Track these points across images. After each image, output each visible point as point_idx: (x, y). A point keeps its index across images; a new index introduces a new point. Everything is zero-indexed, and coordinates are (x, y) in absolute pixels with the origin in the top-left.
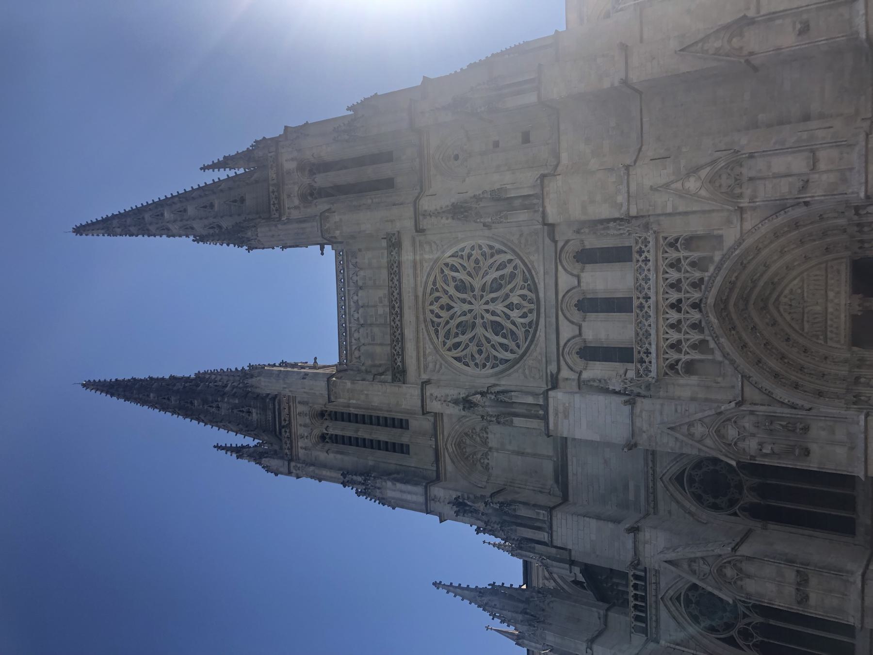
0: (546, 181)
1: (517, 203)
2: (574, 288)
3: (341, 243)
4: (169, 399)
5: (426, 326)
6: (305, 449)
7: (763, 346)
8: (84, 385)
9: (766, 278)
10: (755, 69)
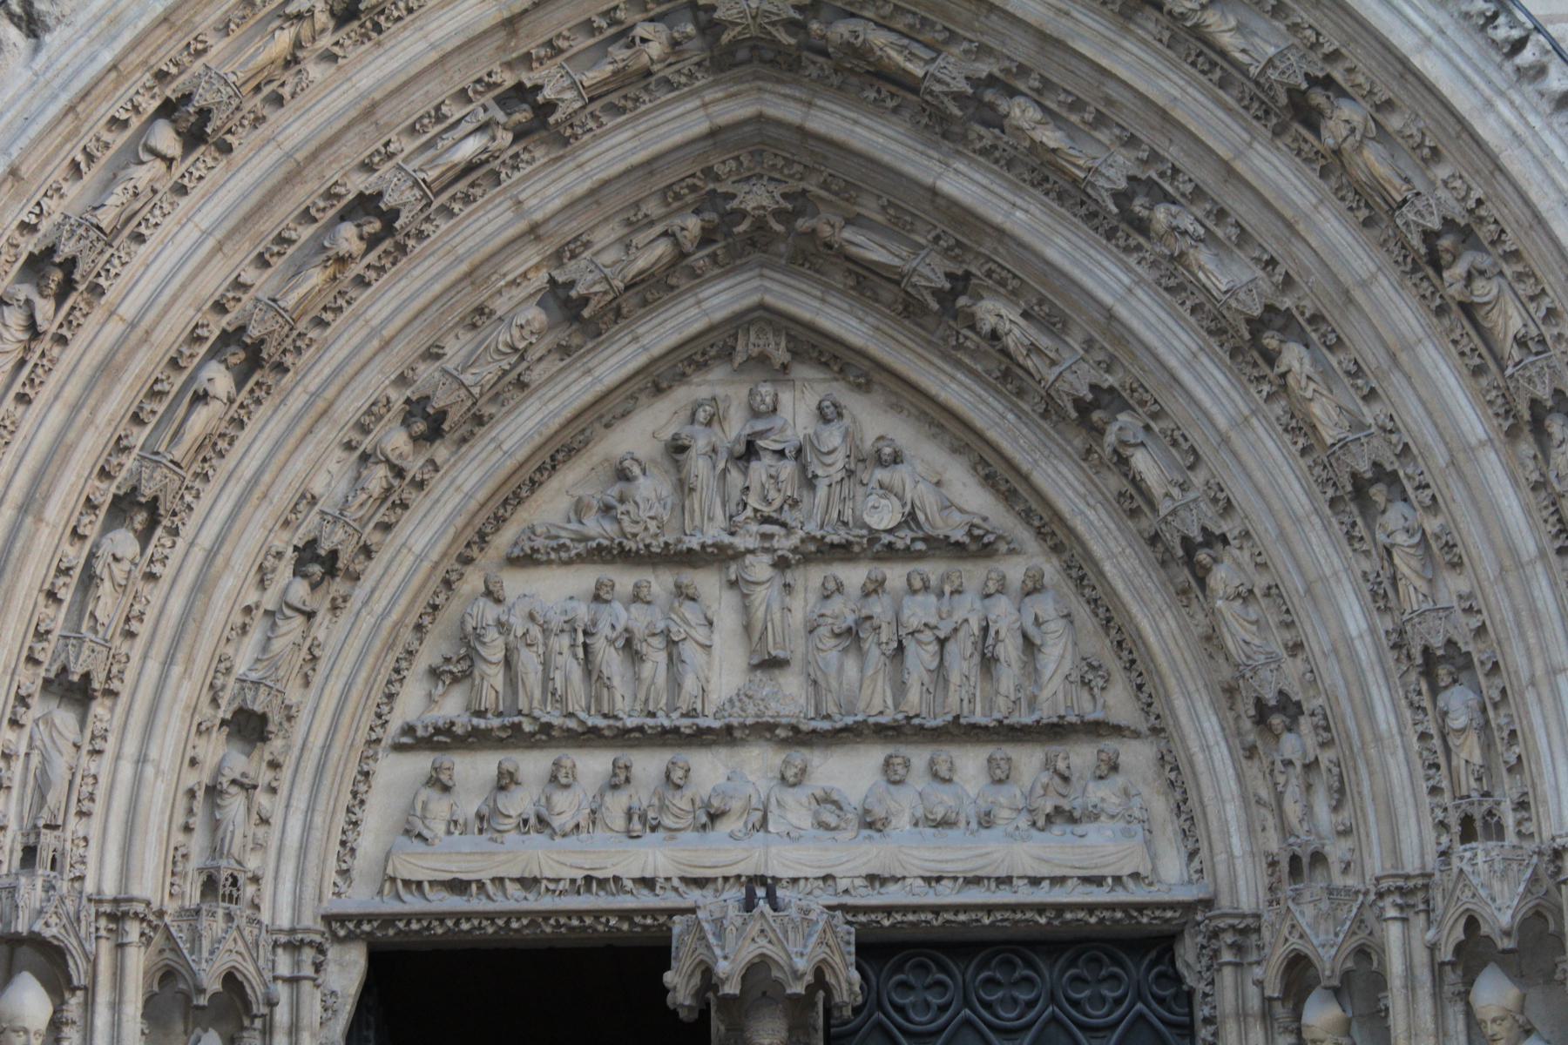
7: (360, 183)
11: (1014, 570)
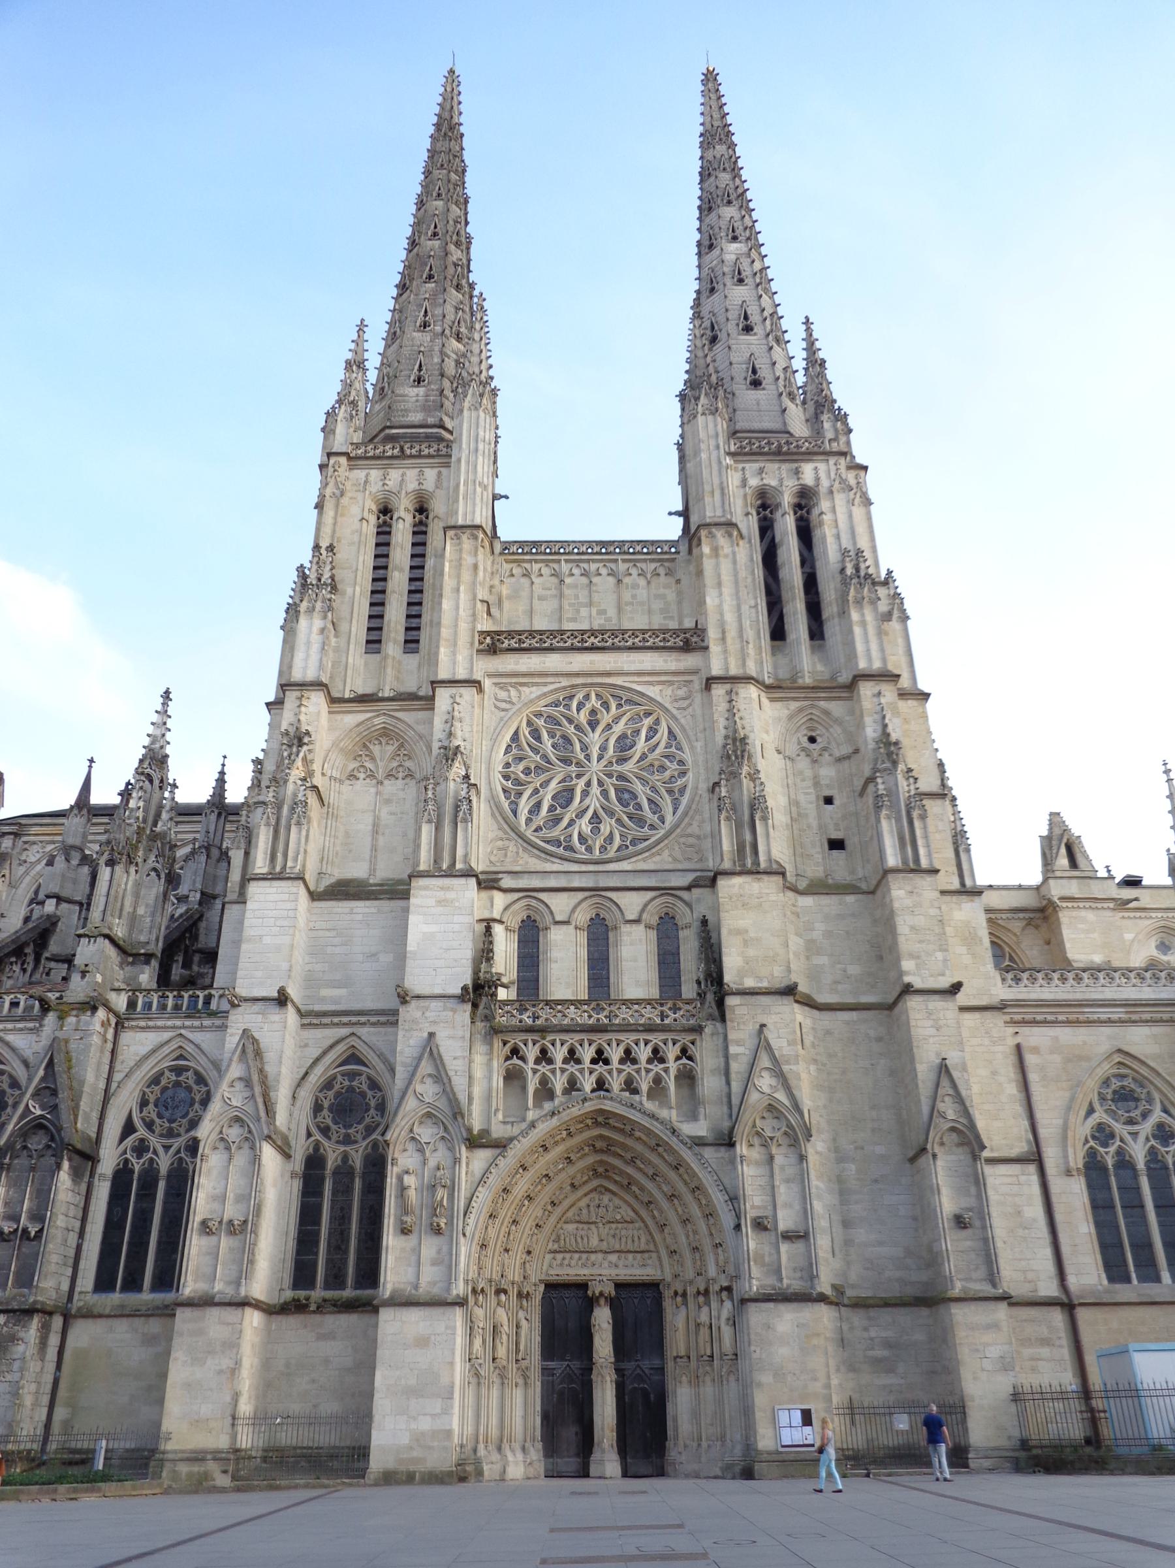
0: (778, 879)
1: (748, 837)
2: (622, 914)
3: (690, 552)
4: (435, 234)
5: (564, 688)
6: (366, 482)
8: (452, 72)
9: (638, 1176)
10: (913, 1160)
11: (637, 1225)
